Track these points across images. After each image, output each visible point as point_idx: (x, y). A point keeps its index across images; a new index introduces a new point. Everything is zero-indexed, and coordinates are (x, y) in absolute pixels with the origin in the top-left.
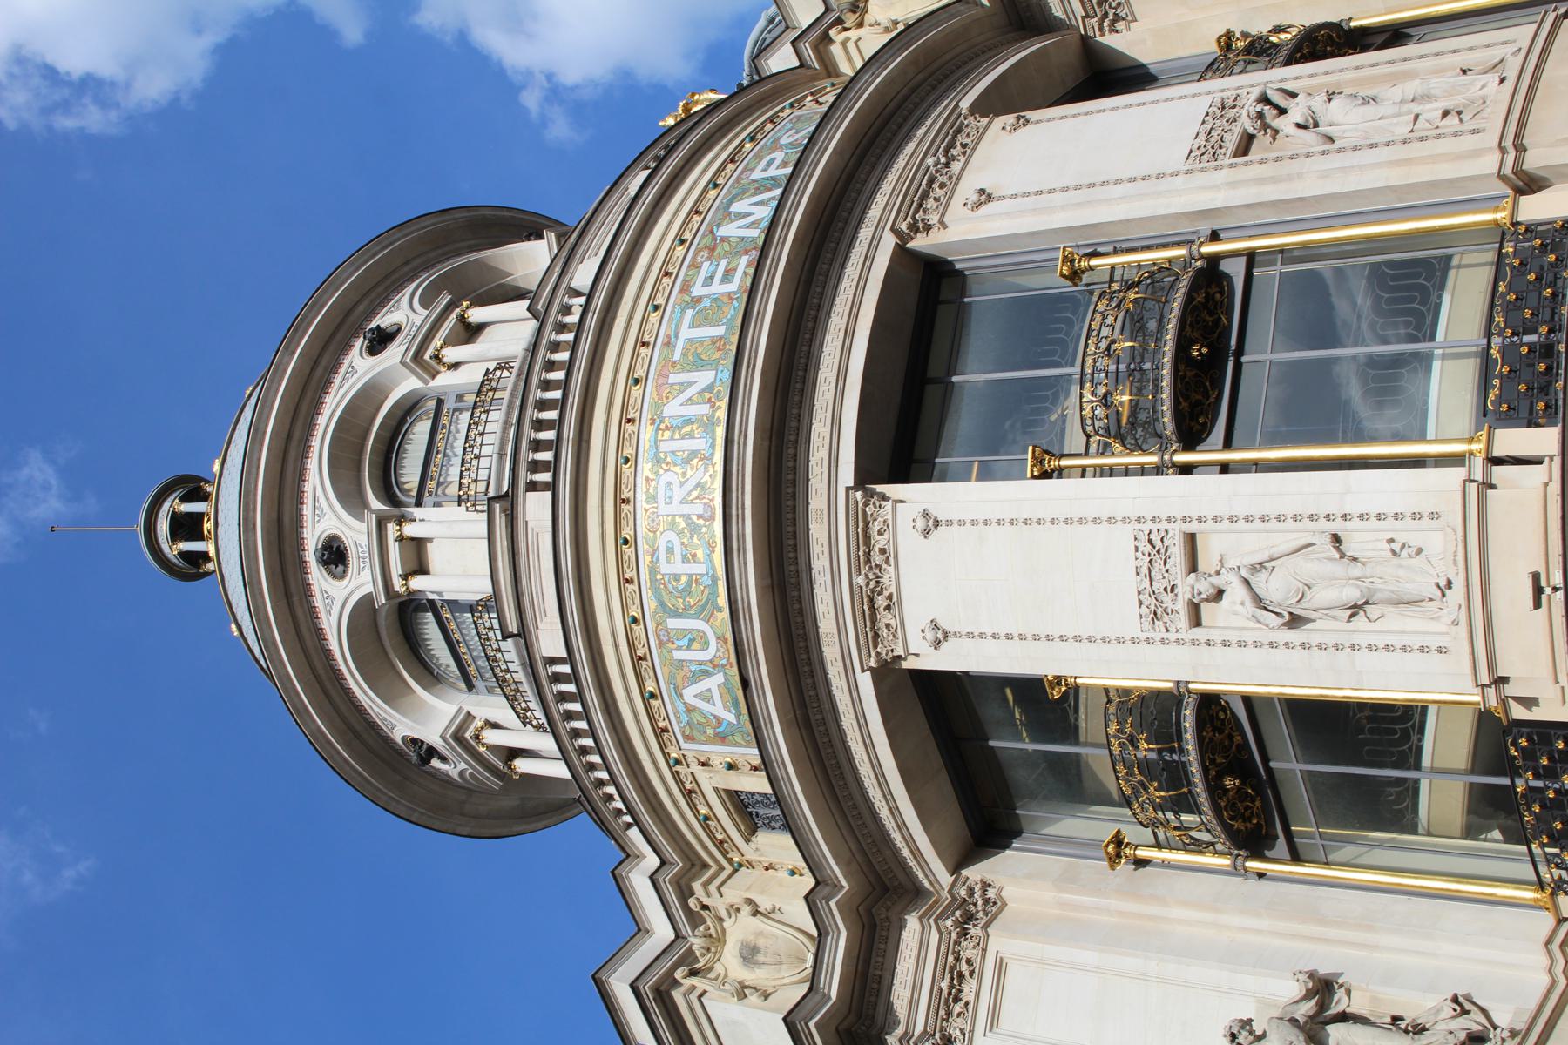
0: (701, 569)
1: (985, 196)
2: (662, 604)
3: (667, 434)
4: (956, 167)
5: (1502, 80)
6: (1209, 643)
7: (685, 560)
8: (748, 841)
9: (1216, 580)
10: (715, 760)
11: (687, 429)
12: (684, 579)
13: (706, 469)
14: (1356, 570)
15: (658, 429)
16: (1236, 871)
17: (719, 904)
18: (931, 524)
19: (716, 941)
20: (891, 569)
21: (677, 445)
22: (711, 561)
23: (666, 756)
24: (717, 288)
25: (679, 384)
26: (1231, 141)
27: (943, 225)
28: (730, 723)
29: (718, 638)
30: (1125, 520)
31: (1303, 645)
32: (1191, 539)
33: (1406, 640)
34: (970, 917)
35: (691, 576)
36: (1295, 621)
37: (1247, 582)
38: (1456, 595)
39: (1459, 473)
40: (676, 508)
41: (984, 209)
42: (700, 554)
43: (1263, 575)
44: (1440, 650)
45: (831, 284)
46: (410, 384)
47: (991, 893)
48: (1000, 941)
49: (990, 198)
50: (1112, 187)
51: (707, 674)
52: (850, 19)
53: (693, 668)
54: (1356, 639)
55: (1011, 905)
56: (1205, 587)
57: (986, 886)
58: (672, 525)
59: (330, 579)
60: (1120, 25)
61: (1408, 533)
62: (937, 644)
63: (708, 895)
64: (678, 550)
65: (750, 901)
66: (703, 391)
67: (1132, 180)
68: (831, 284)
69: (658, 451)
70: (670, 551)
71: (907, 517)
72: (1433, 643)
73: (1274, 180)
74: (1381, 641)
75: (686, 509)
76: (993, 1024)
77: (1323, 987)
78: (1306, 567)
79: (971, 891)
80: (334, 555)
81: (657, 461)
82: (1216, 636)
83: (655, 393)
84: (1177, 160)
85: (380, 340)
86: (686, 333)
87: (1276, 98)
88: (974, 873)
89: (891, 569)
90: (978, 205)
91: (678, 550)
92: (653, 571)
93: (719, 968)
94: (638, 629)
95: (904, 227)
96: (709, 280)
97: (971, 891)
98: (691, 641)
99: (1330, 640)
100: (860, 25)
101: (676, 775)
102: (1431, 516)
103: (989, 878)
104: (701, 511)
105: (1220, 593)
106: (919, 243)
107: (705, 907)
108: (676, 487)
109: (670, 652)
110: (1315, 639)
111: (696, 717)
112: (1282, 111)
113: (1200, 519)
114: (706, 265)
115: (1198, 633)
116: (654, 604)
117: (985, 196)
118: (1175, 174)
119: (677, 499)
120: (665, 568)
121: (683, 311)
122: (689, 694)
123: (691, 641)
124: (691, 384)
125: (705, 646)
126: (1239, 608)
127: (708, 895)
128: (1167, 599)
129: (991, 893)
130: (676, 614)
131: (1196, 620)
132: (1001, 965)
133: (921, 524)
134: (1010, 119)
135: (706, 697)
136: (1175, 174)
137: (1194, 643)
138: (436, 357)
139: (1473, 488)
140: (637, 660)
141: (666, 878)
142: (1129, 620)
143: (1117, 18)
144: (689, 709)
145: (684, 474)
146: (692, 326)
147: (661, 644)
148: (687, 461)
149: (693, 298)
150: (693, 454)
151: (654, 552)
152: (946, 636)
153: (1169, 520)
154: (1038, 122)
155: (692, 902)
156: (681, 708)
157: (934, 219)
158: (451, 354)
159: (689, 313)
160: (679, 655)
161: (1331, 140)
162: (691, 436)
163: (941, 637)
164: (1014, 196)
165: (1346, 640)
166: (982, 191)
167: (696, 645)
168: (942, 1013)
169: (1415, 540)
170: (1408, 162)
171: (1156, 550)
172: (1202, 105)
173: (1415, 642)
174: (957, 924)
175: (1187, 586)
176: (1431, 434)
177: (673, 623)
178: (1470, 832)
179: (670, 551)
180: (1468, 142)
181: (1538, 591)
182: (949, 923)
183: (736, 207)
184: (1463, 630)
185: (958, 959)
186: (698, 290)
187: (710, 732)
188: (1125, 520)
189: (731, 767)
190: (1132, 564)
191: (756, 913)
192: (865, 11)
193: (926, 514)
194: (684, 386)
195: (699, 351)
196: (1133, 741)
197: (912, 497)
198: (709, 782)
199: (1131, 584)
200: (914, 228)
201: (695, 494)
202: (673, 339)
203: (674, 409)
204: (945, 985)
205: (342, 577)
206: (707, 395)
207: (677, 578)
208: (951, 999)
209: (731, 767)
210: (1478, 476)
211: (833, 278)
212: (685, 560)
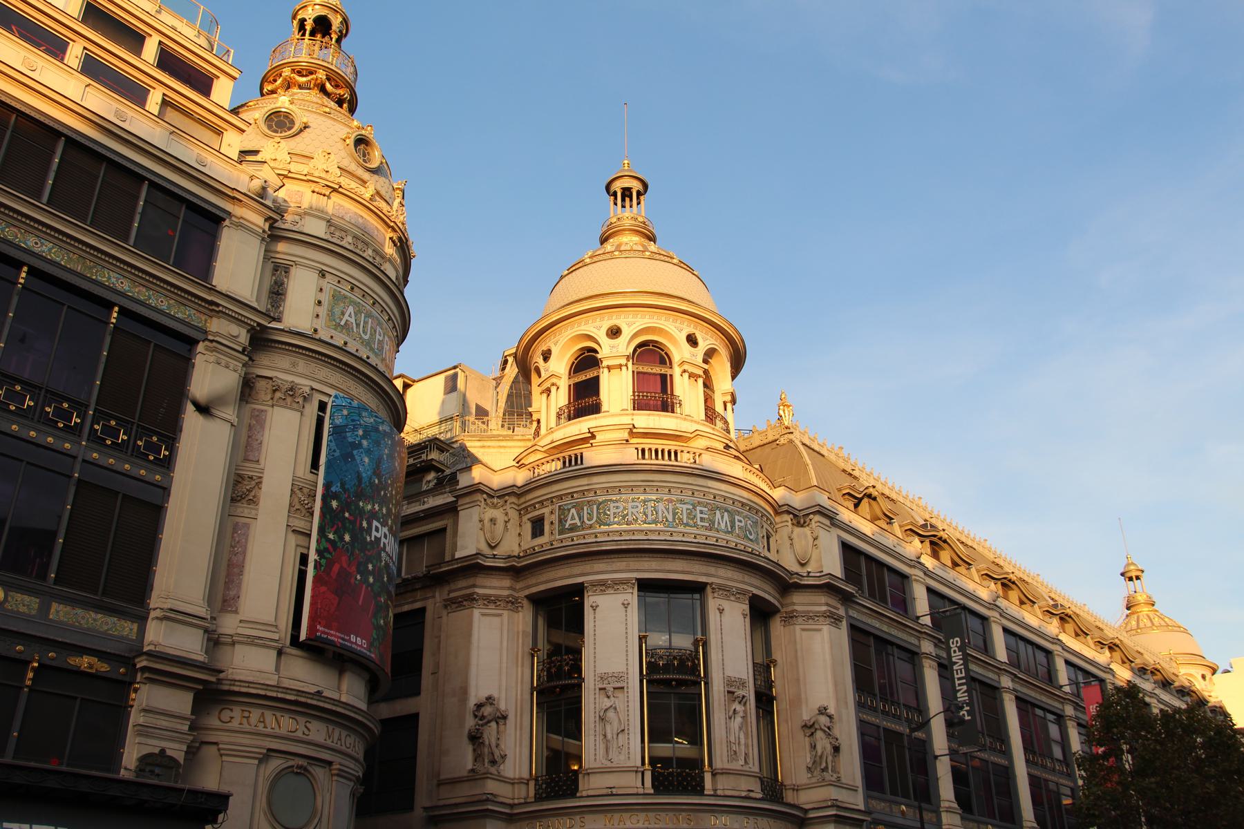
0: (612, 520)
1: (721, 611)
2: (600, 504)
3: (653, 505)
4: (732, 598)
5: (742, 766)
6: (595, 694)
7: (614, 513)
8: (528, 519)
9: (612, 696)
10: (553, 516)
11: (654, 513)
12: (608, 513)
13: (642, 521)
14: (615, 737)
15: (655, 501)
16: (532, 688)
17: (508, 506)
18: (626, 606)
19: (495, 506)
20: (612, 592)
21: (650, 509)
22: (615, 524)
23: (553, 497)
24: (699, 516)
26: (732, 689)
27: (714, 598)
28: (565, 525)
29: (591, 525)
30: (627, 669)
31: (595, 721)
32: (623, 688)
33: (598, 750)
34: (513, 603)
35: (609, 515)
36: (602, 719)
37: (611, 706)
38: (609, 764)
39: (640, 765)
40: (631, 510)
41: (717, 611)
42: (616, 519)
43: (613, 711)
44: (595, 759)
46: (676, 358)
47: (520, 609)
48: (506, 613)
49: (721, 613)
50: (721, 653)
51: (580, 519)
52: (795, 522)
53: (582, 514)
54: (597, 736)
55: (516, 615)
56: (610, 693)
57: (522, 607)
58: (625, 508)
59: (606, 329)
60: (783, 623)
61: (625, 751)
62: (592, 606)
63: (510, 503)
64: (618, 510)
65: (509, 520)
66: (666, 518)
67: (723, 660)
69: (648, 502)
70: (617, 508)
71: (628, 597)
72: (597, 757)
73: (720, 705)
74: (597, 742)
75: (630, 514)
76: (483, 615)
77: (505, 718)
78: (616, 724)
79: (520, 603)
80: (615, 332)
81: (645, 501)
82: (597, 696)
83: (666, 498)
84: (729, 673)
85: (692, 341)
86: (685, 507)
87: (744, 700)
88: (525, 602)
89: (612, 592)
90: (719, 609)
91: (618, 510)
92: (611, 500)
93: (488, 509)
94: (592, 494)
95: (714, 586)
96: (701, 512)
97: (520, 603)
98: (590, 514)
99: (597, 729)
100: (793, 524)
101: (547, 499)
102: (629, 757)
103: (524, 608)
104: (629, 520)
105: (608, 697)
106: (709, 589)
107: (506, 502)
108: (636, 510)
109: (586, 505)
110: (597, 725)
111: (566, 512)
112: (740, 703)
113: (628, 692)
114: (706, 509)
115: (597, 690)
116: (600, 500)
117: (721, 611)
118: (724, 674)
119: (633, 510)
120: (612, 505)
121: (692, 505)
122: (573, 511)
123: (590, 514)
125: (589, 520)
126: (604, 705)
127: (510, 503)
128: (606, 682)
129: (520, 609)
130: (598, 509)
131: (600, 689)
132: (500, 615)
133: (626, 602)
134: (748, 612)
135: (573, 518)
136: (724, 674)
137: (595, 689)
138: (685, 371)
139: (636, 769)
140: (583, 492)
141: (515, 490)
142: (602, 669)
143: (785, 621)
144: (569, 510)
145: (640, 513)
146: (687, 509)
147: (588, 502)
148: (645, 514)
150: (647, 516)
151: (617, 501)
152: (595, 610)
153: (627, 682)
154: (745, 622)
155: (507, 497)
156: (569, 507)
157: (716, 595)
158: (686, 375)
159: (691, 507)
160: (585, 508)
161: (730, 718)
162: (652, 515)
163: (594, 608)
164: (721, 621)
165: (597, 734)
166: (723, 610)
167: (589, 516)
168: (484, 598)
169: (623, 752)
170: (721, 743)
171: (619, 677)
172: (744, 677)
173: (597, 753)
174: (510, 601)
175: (610, 688)
176: (651, 745)
177: (595, 507)
178: (548, 748)
179: (617, 508)
180: (725, 759)
181: (611, 788)
182: (510, 599)
183: (726, 514)
184: (600, 766)
185: (500, 601)
186: (698, 508)
187: (562, 517)
188: (627, 669)
189: (552, 523)
190: (615, 671)
191: (506, 522)
192: (797, 526)
193: (628, 604)
194: (668, 510)
196: (567, 664)
197: (632, 596)
198: (546, 511)
199: (610, 671)
200: (713, 589)
201: (634, 517)
203: (661, 506)
204: (493, 598)
205: (607, 335)
206: (665, 520)
207: (609, 510)
208: (490, 600)
209: (552, 523)
210: (639, 769)
212: (614, 513)
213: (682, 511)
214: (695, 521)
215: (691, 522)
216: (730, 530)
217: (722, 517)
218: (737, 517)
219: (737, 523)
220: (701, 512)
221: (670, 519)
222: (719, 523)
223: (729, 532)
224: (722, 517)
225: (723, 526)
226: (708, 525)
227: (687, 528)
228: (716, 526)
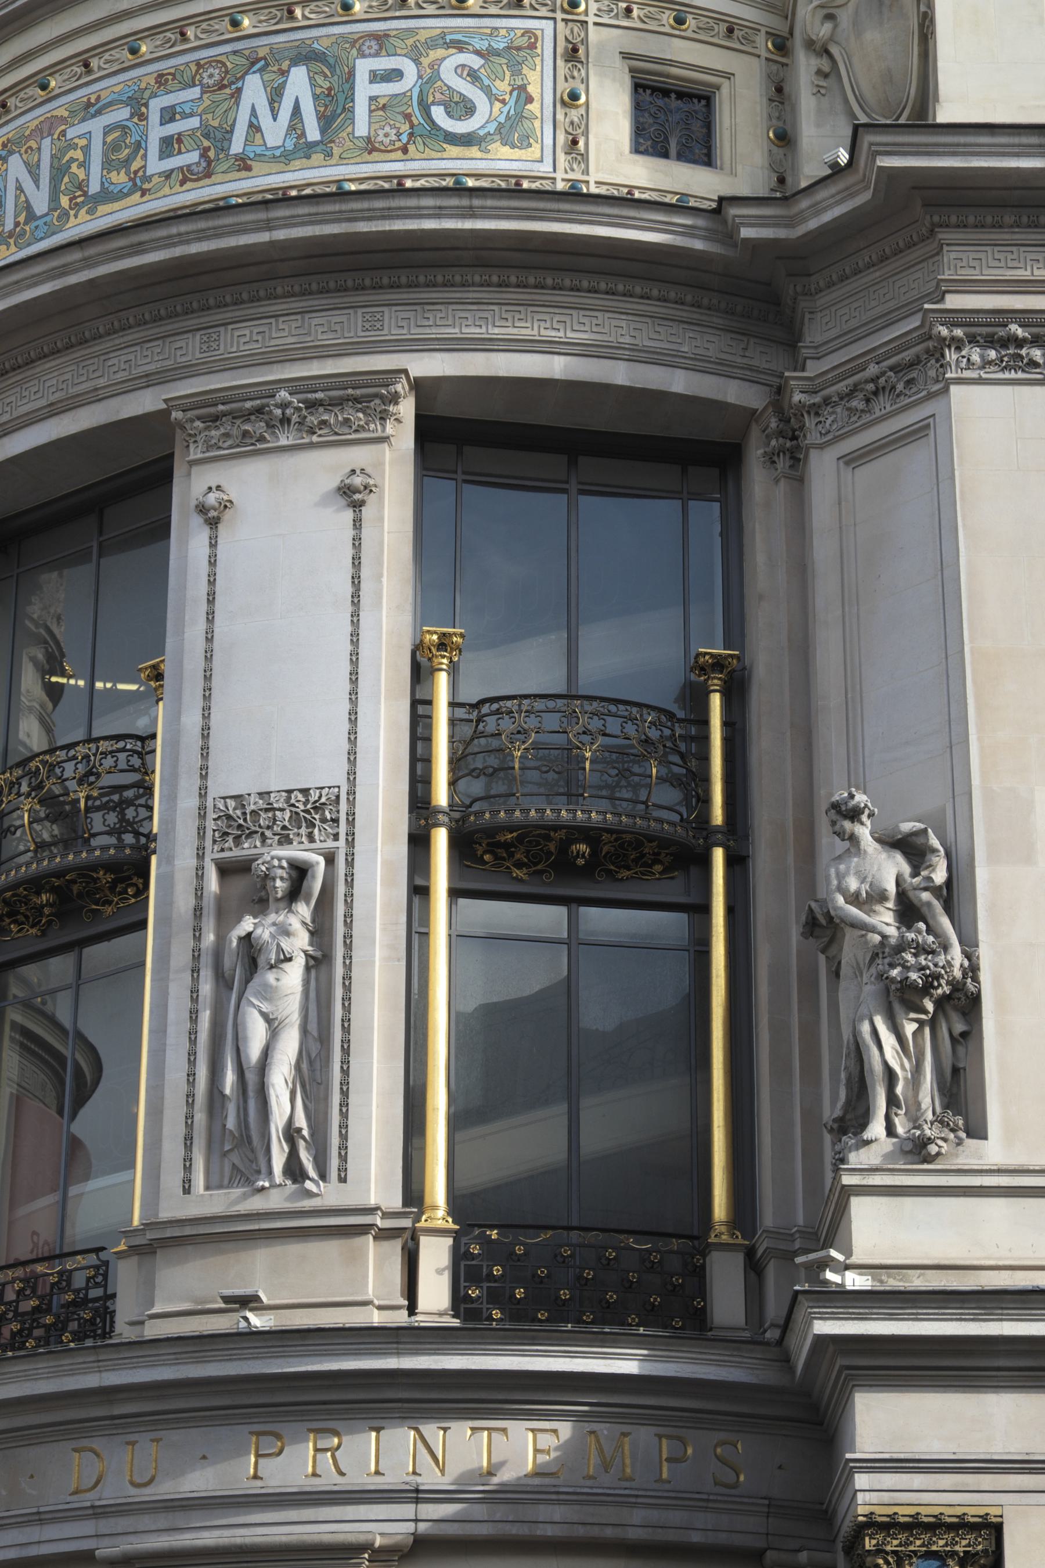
25: (39, 160)
45: (117, 342)
68: (117, 342)
114: (196, 92)
124: (36, 181)
149: (146, 105)
186: (156, 105)
195: (74, 168)
202: (92, 110)
211: (126, 339)
213: (86, 150)
214: (135, 165)
215: (120, 178)
216: (313, 134)
217: (275, 96)
218: (363, 67)
219: (364, 90)
220: (169, 115)
221: (41, 206)
222: (254, 128)
223: (306, 149)
224: (275, 96)
225: (275, 133)
226: (193, 157)
227: (102, 209)
228: (237, 146)
